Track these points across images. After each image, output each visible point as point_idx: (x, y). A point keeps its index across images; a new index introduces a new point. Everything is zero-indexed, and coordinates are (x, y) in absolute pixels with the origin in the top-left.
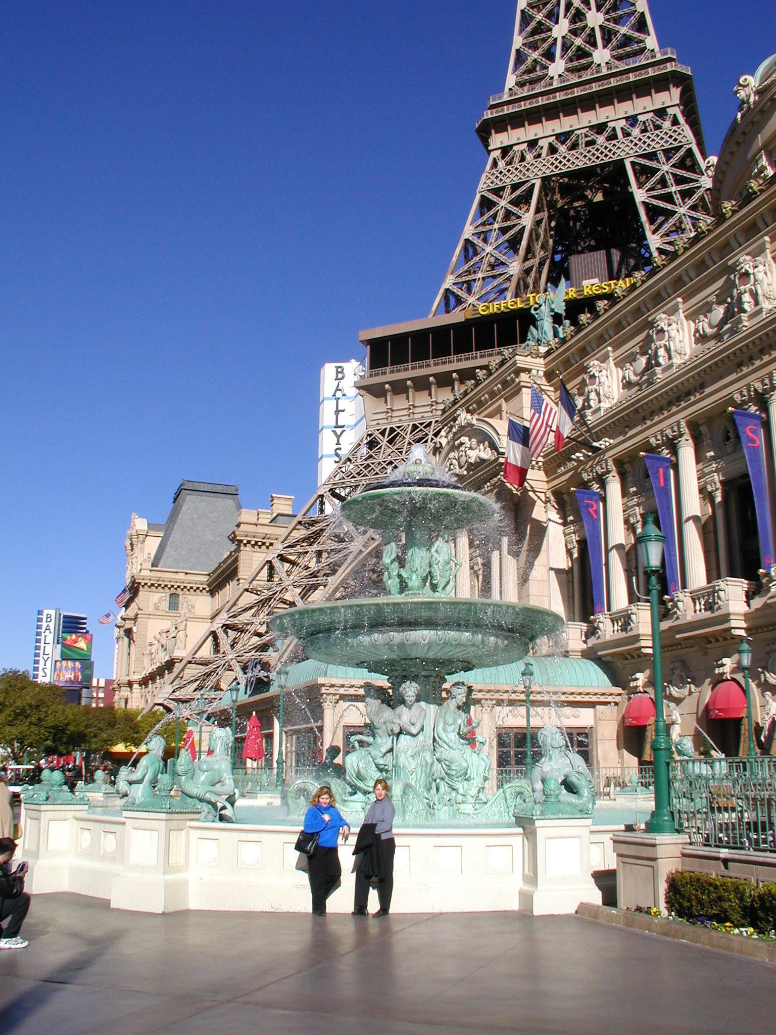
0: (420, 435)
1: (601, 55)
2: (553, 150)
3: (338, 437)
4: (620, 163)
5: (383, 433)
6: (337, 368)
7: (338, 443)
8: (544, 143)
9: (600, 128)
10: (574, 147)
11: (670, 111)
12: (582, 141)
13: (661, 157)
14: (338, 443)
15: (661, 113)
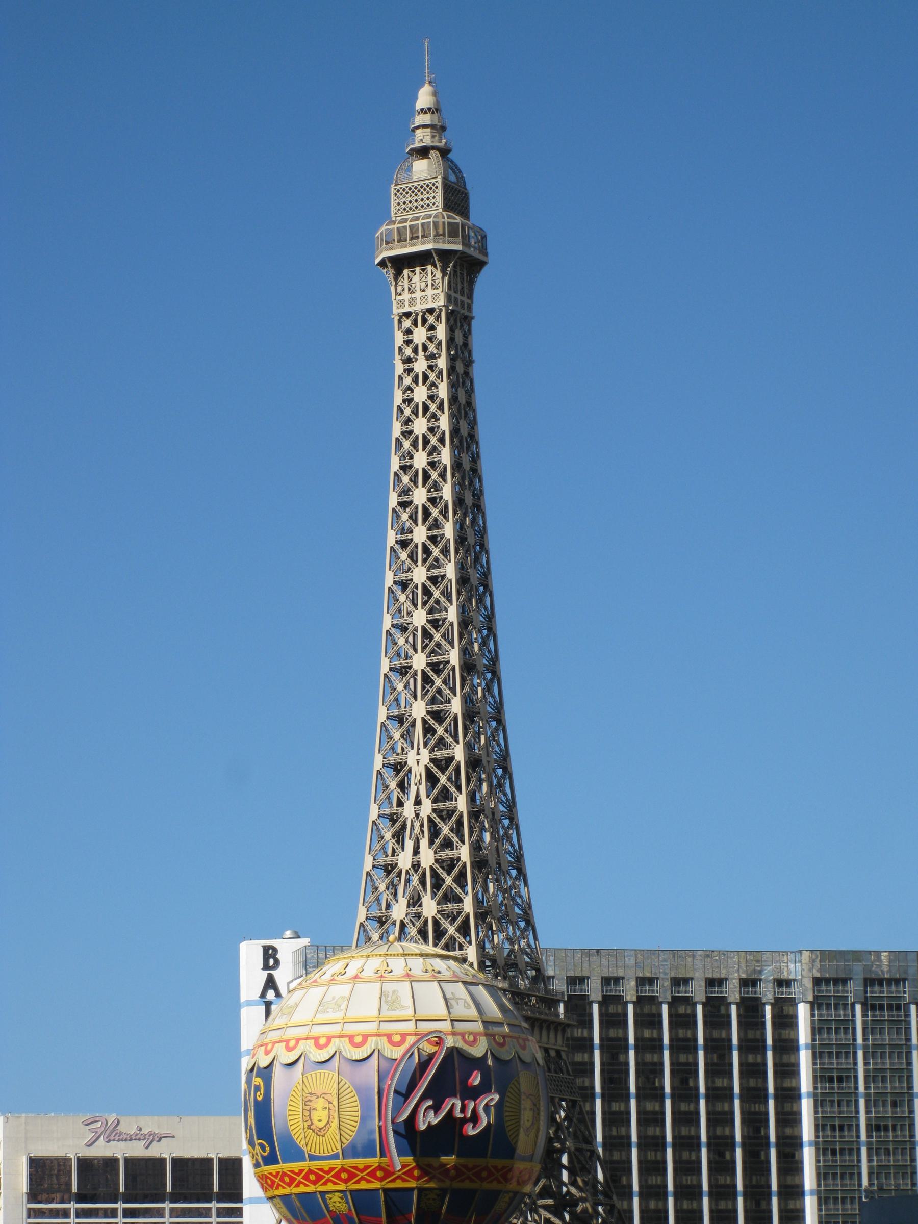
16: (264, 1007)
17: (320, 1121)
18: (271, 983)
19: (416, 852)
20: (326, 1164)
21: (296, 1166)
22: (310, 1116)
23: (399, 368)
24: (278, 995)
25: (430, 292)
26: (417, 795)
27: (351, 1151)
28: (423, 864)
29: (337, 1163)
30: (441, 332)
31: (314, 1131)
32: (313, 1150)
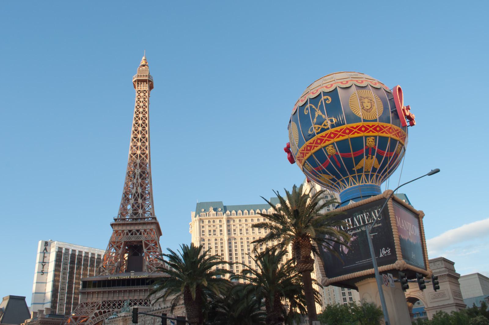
0: (93, 305)
1: (140, 211)
2: (127, 234)
3: (43, 266)
4: (141, 242)
5: (85, 303)
6: (46, 242)
7: (43, 268)
8: (125, 231)
9: (138, 231)
10: (132, 234)
11: (154, 230)
12: (134, 233)
13: (150, 241)
14: (43, 268)
15: (151, 230)
16: (43, 254)
17: (367, 106)
18: (46, 249)
19: (137, 189)
20: (371, 124)
21: (355, 125)
22: (362, 104)
23: (137, 99)
24: (47, 251)
25: (145, 87)
26: (137, 178)
27: (381, 120)
28: (138, 192)
29: (376, 124)
30: (147, 94)
31: (365, 110)
32: (365, 117)
